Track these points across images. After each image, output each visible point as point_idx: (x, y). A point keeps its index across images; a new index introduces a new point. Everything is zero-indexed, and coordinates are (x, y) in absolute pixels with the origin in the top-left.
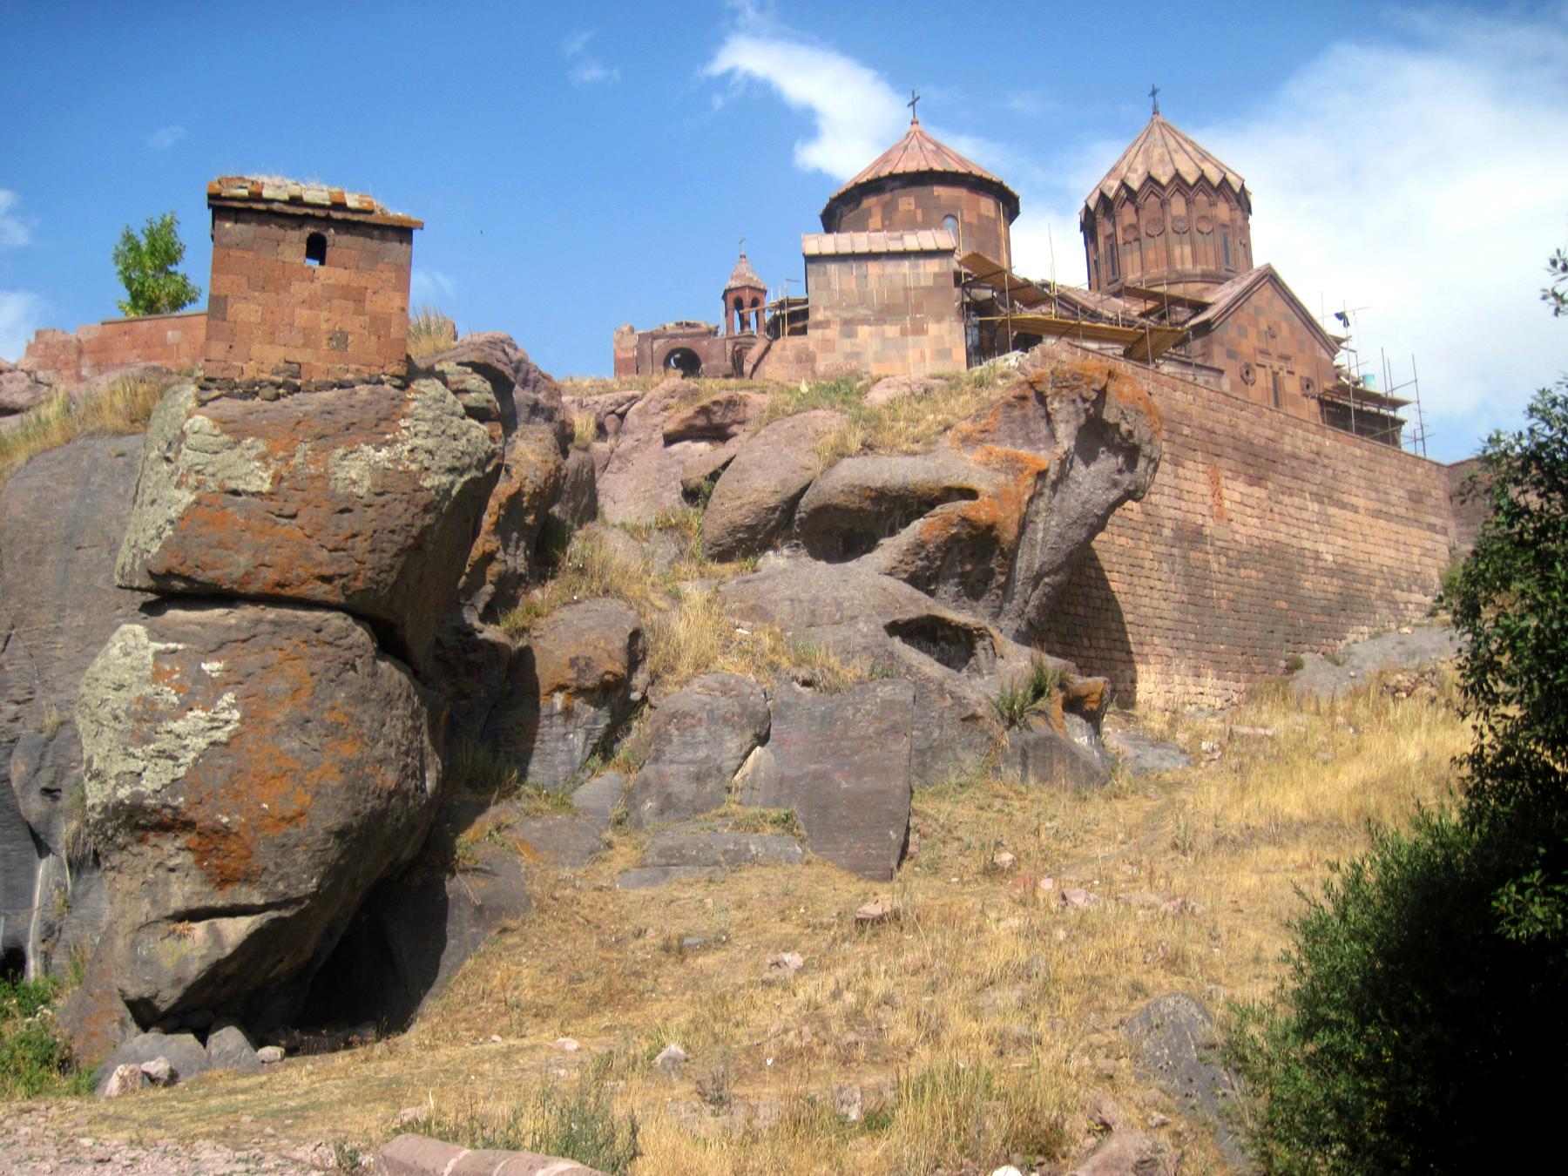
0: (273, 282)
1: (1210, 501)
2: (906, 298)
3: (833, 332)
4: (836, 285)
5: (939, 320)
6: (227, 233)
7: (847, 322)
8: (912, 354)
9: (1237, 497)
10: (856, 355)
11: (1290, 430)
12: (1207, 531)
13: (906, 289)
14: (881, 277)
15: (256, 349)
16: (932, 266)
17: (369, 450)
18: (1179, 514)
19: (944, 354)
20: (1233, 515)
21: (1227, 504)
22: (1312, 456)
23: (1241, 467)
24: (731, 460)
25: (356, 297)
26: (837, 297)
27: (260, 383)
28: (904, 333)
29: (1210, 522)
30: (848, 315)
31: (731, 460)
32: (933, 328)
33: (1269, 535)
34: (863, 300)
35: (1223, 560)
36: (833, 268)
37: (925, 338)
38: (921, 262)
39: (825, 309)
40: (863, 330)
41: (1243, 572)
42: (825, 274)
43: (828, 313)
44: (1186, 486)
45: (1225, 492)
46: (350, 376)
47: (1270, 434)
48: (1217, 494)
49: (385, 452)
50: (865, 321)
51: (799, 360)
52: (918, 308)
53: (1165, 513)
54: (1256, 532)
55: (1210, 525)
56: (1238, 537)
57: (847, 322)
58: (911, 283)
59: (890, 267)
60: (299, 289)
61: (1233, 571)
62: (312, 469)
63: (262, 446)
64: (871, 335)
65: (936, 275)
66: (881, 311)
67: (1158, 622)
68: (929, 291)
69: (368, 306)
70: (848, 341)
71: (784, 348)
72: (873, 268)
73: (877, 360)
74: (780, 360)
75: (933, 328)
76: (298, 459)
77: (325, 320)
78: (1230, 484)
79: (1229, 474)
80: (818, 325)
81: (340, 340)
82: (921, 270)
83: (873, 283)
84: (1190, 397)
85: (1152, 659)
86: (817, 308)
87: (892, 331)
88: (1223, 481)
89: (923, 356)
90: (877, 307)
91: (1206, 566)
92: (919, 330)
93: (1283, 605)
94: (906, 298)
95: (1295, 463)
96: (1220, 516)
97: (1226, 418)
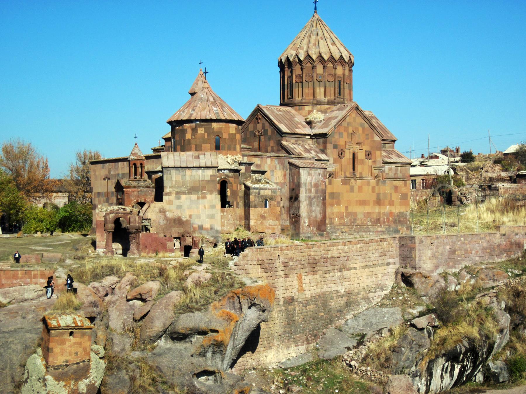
0: (63, 342)
1: (297, 287)
2: (200, 184)
3: (173, 197)
4: (174, 179)
5: (211, 193)
6: (53, 334)
7: (177, 193)
8: (201, 206)
9: (308, 281)
10: (179, 207)
11: (331, 248)
12: (295, 297)
13: (199, 181)
14: (191, 176)
15: (59, 358)
16: (210, 172)
17: (84, 380)
18: (285, 295)
19: (213, 207)
20: (305, 288)
21: (304, 285)
22: (338, 255)
23: (311, 269)
24: (149, 311)
25: (80, 344)
26: (174, 184)
27: (60, 365)
28: (198, 198)
29: (297, 294)
30: (178, 190)
31: (149, 311)
32: (209, 196)
33: (319, 291)
34: (184, 184)
35: (301, 305)
36: (173, 171)
37: (206, 200)
38: (206, 170)
39: (170, 187)
40: (183, 197)
41: (308, 307)
42: (170, 174)
43: (171, 189)
44: (290, 284)
45: (304, 281)
46: (78, 361)
47: (323, 253)
48: (301, 283)
49: (88, 380)
50: (184, 193)
51: (160, 211)
52: (204, 188)
53: (281, 296)
54: (314, 291)
55: (297, 295)
56: (307, 296)
57: (177, 193)
58: (202, 179)
59: (194, 172)
60: (68, 344)
61: (304, 308)
62: (75, 388)
63: (64, 383)
64: (186, 199)
65: (211, 176)
66: (190, 189)
67: (276, 334)
68: (208, 182)
69: (82, 346)
70: (177, 201)
71: (155, 207)
72: (188, 172)
73: (188, 209)
74: (153, 211)
75: (209, 196)
76: (72, 387)
77: (74, 349)
78: (306, 278)
79: (306, 274)
80: (167, 194)
81: (76, 353)
82: (206, 174)
83: (188, 178)
84: (294, 251)
85: (273, 347)
86: (167, 187)
87: (194, 197)
88: (303, 277)
89: (205, 207)
90: (189, 188)
91: (294, 310)
92: (204, 197)
93: (322, 314)
94: (200, 184)
95: (332, 260)
96: (301, 290)
97: (306, 254)
